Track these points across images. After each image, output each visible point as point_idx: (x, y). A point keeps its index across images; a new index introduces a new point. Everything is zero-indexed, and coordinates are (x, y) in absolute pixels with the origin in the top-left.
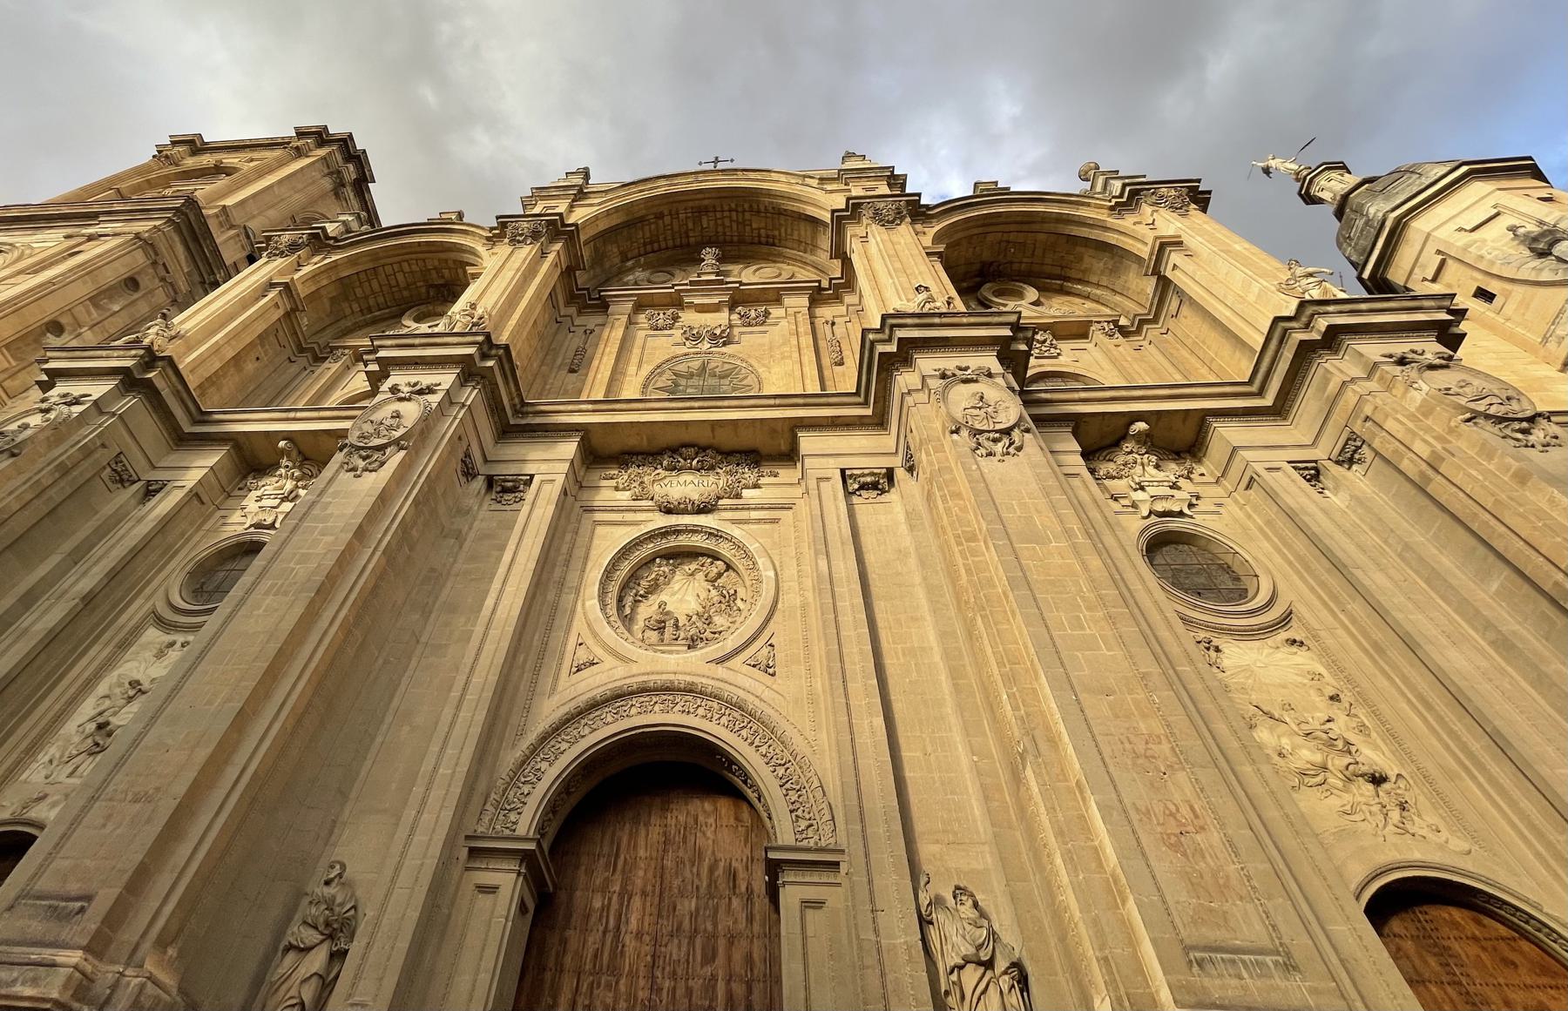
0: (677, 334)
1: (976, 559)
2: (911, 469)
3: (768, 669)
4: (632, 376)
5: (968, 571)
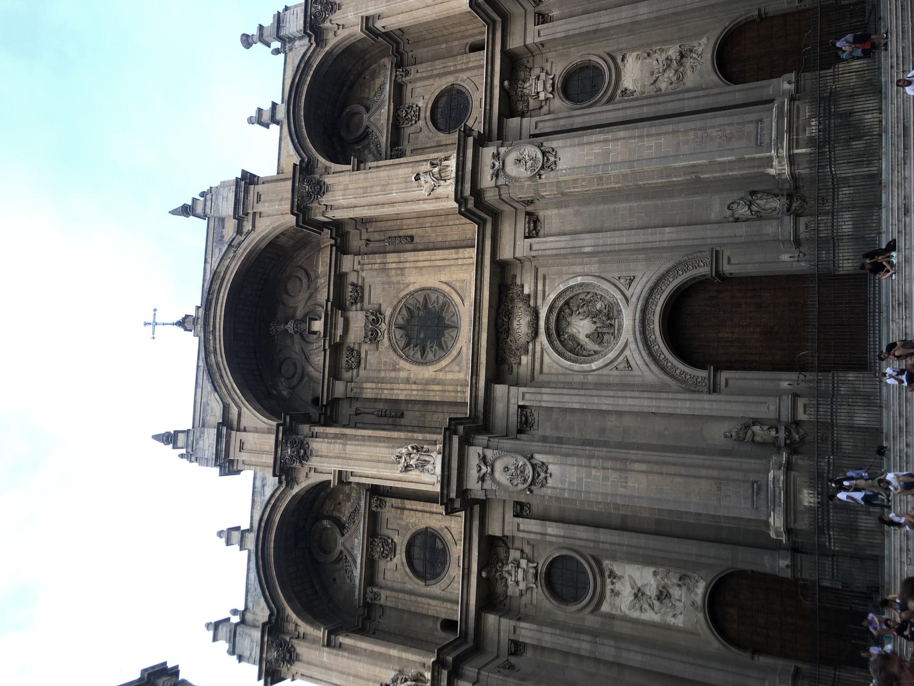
0: (365, 347)
1: (612, 179)
2: (532, 202)
3: (632, 280)
4: (410, 374)
5: (617, 183)
